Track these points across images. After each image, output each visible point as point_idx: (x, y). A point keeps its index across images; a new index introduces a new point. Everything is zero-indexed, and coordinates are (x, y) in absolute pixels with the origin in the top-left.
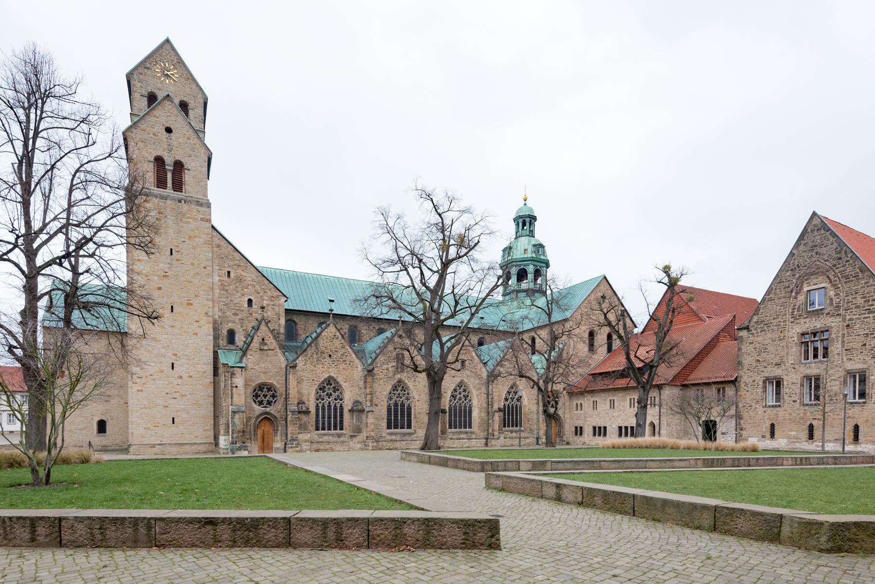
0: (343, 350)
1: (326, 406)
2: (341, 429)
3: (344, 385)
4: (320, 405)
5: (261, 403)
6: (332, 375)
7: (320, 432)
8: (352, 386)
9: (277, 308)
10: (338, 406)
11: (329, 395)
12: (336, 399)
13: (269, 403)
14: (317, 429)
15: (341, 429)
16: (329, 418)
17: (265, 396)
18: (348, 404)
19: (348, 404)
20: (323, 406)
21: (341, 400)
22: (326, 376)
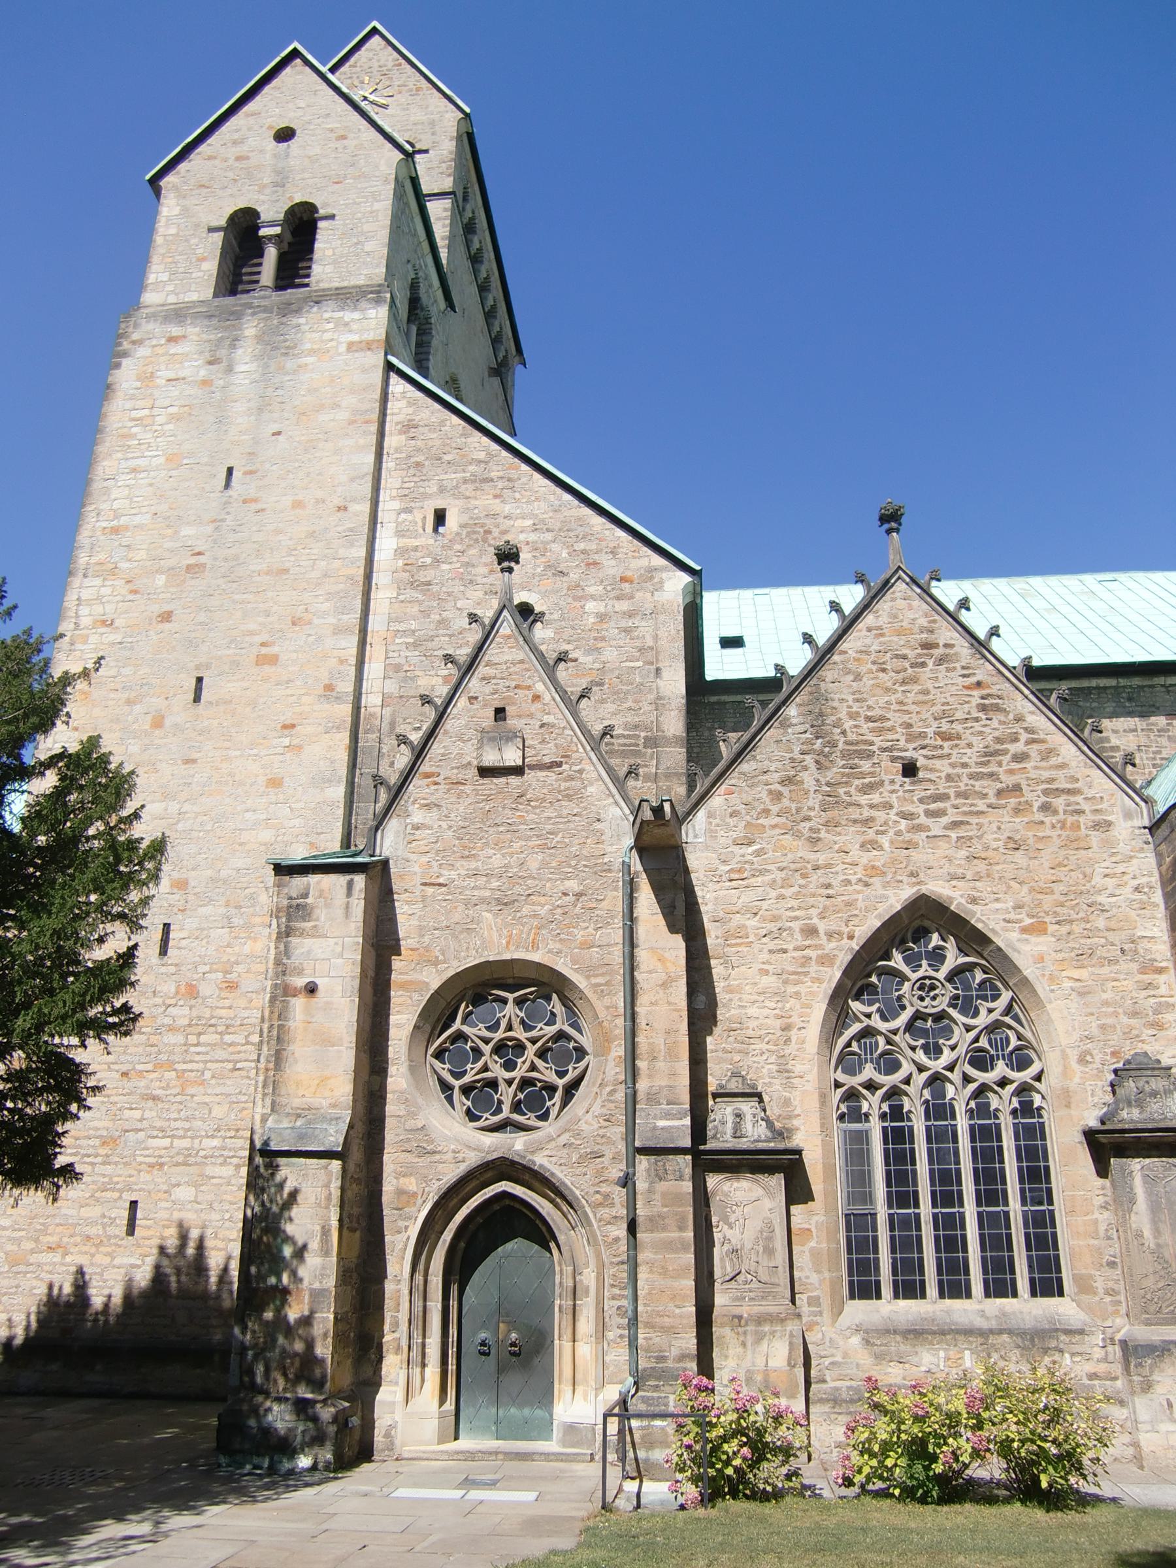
0: (995, 726)
1: (914, 1104)
2: (1048, 1284)
3: (1026, 952)
4: (872, 1104)
5: (480, 1094)
6: (938, 888)
7: (890, 1308)
8: (1083, 957)
9: (645, 629)
10: (1003, 1103)
11: (929, 1030)
12: (981, 1061)
13: (535, 1099)
14: (864, 1287)
15: (1048, 1284)
16: (947, 1196)
17: (508, 1051)
18: (1074, 1102)
19: (1074, 1102)
20: (897, 1113)
21: (1022, 1063)
22: (896, 899)
